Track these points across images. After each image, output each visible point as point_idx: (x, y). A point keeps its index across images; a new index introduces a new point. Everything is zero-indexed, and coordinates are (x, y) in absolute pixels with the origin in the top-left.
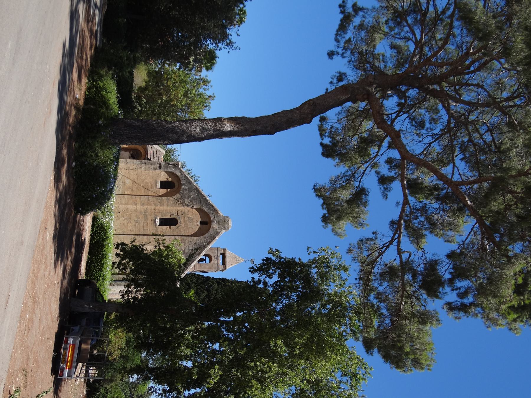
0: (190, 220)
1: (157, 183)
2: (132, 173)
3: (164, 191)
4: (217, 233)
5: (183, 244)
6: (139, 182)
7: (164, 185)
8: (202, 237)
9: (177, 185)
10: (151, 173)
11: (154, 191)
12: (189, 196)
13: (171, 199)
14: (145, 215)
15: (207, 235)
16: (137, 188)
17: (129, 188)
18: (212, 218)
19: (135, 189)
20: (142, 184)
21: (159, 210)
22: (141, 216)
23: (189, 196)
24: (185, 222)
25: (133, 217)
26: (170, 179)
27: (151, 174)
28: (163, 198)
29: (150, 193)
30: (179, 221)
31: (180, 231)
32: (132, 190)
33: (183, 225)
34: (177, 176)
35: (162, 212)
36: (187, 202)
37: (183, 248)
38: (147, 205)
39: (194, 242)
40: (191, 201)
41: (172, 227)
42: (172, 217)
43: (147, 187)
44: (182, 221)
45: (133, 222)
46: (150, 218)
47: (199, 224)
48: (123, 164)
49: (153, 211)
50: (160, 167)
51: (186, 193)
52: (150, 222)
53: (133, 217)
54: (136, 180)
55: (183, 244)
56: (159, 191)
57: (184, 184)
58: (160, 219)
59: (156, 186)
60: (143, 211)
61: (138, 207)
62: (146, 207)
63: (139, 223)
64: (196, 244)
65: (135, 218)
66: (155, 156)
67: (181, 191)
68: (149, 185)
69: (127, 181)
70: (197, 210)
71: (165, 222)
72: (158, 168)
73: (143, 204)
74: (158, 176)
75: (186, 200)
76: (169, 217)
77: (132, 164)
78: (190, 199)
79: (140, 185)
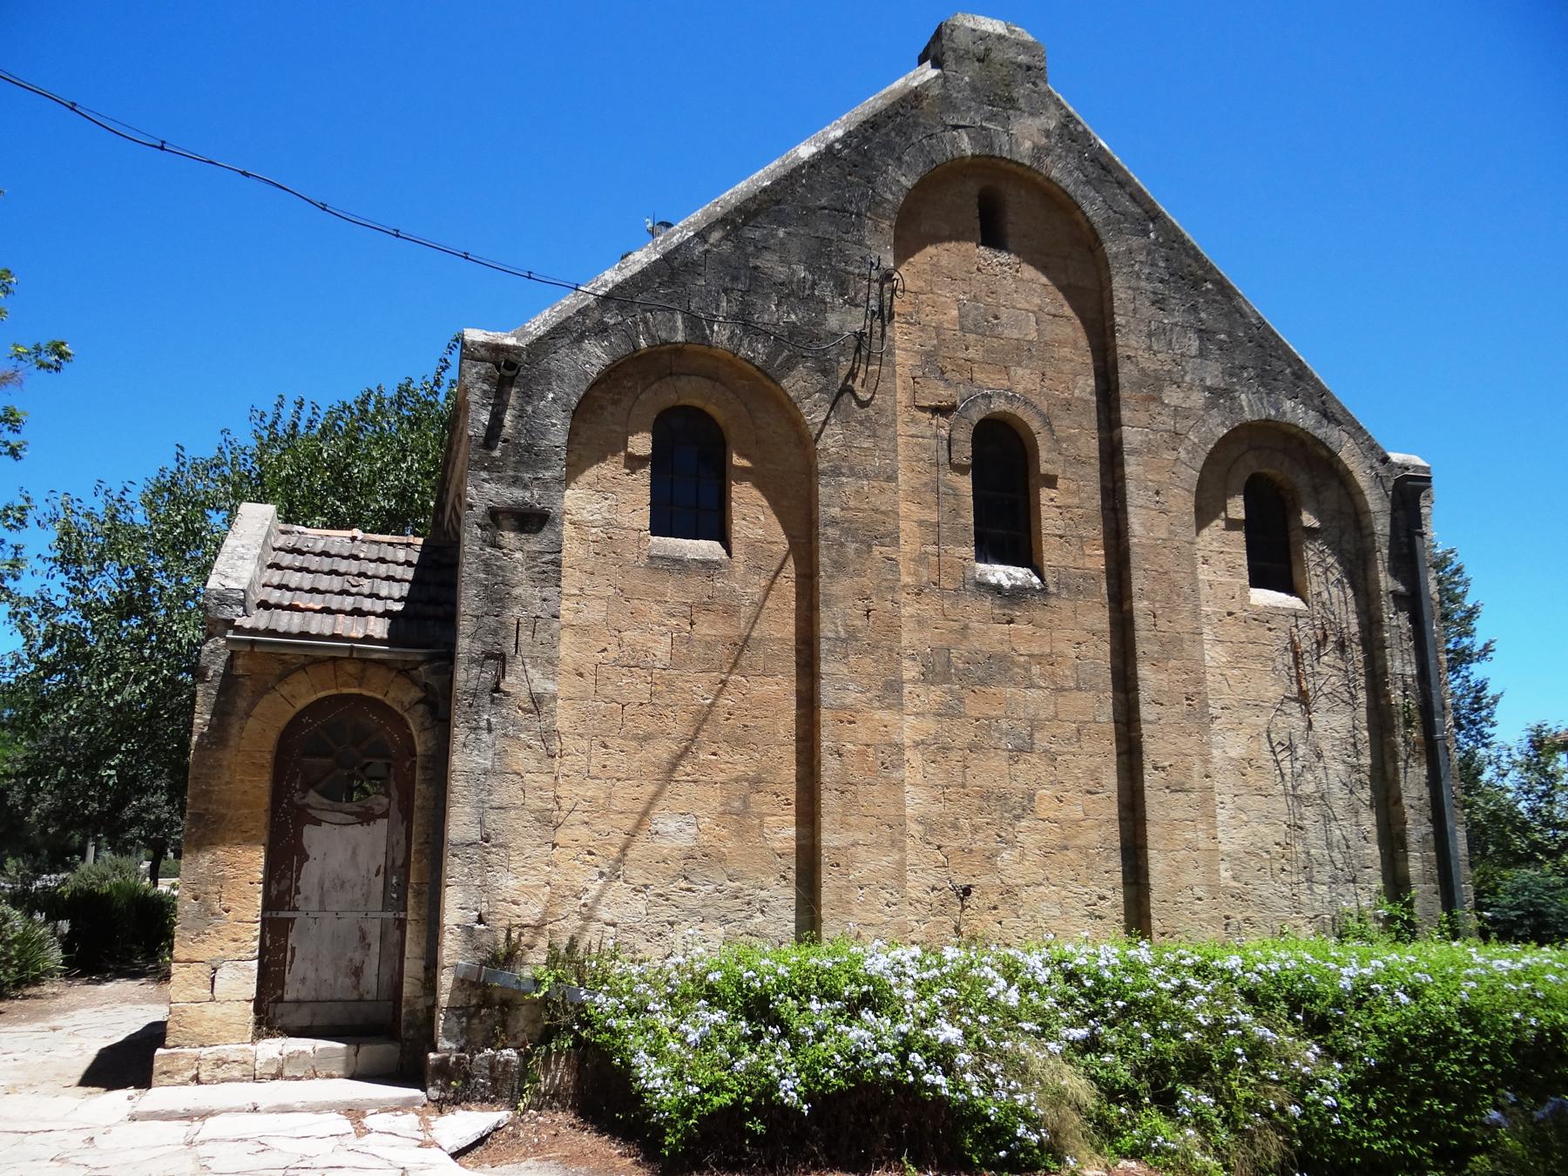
0: (982, 324)
1: (678, 564)
2: (591, 789)
3: (752, 514)
4: (1070, 134)
5: (1172, 396)
6: (679, 727)
7: (688, 499)
8: (1111, 248)
9: (689, 392)
10: (582, 600)
11: (756, 592)
12: (791, 293)
13: (831, 442)
14: (963, 676)
15: (1093, 208)
16: (738, 742)
17: (739, 816)
18: (966, 146)
19: (741, 763)
20: (700, 688)
21: (921, 559)
22: (973, 706)
23: (791, 293)
25: (991, 770)
26: (641, 444)
27: (594, 612)
28: (829, 509)
29: (781, 627)
30: (999, 405)
31: (1067, 405)
32: (756, 783)
33: (1024, 379)
34: (610, 377)
35: (935, 533)
36: (844, 320)
37: (1198, 399)
38: (895, 656)
39: (1147, 310)
40: (841, 286)
41: (1045, 468)
42: (964, 453)
43: (721, 652)
44: (989, 380)
45: (1031, 770)
46: (989, 634)
47: (1004, 257)
48: (508, 884)
49: (928, 607)
50: (531, 520)
51: (772, 313)
52: (1020, 637)
53: (991, 770)
54: (662, 750)
55: (1172, 396)
56: (752, 545)
57: (693, 322)
58: (982, 556)
59: (707, 565)
60: (935, 695)
61: (909, 728)
62: (910, 671)
63: (1035, 725)
64: (1159, 302)
65: (998, 762)
66: (307, 581)
67: (759, 351)
68: (706, 628)
69: (674, 830)
70: (904, 252)
71: (1006, 526)
72: (534, 543)
73: (892, 690)
74: (608, 544)
75: (833, 321)
76: (965, 484)
77: (506, 793)
78: (825, 290)
79: (703, 717)
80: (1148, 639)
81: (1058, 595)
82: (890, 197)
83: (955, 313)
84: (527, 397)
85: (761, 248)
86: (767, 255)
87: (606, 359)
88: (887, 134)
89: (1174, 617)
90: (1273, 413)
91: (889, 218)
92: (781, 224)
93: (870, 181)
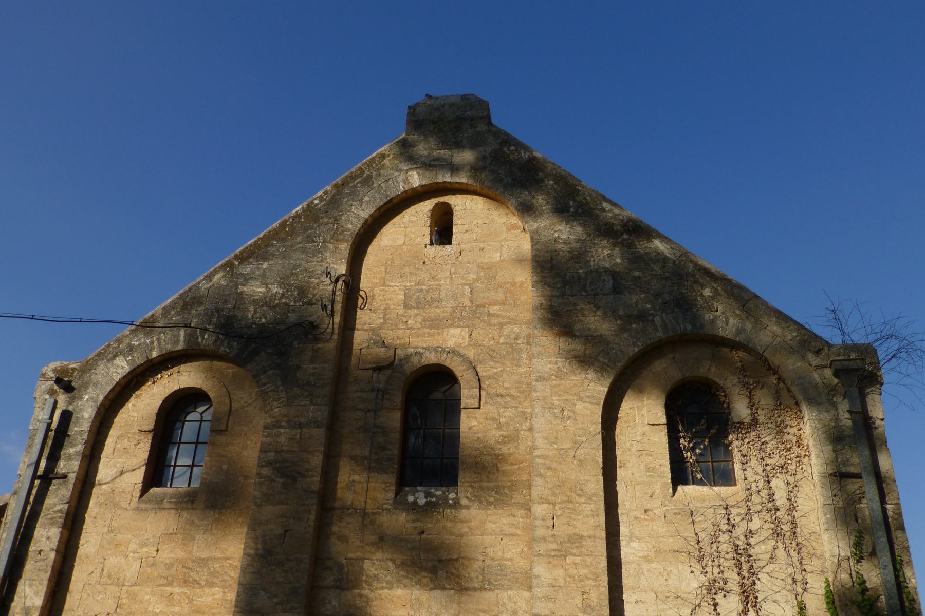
24: (437, 324)
33: (454, 337)
80: (544, 539)
81: (468, 508)
82: (350, 226)
83: (402, 297)
84: (71, 401)
85: (247, 279)
86: (252, 282)
87: (127, 369)
88: (355, 187)
89: (573, 516)
90: (689, 327)
91: (347, 241)
92: (265, 259)
93: (336, 220)
